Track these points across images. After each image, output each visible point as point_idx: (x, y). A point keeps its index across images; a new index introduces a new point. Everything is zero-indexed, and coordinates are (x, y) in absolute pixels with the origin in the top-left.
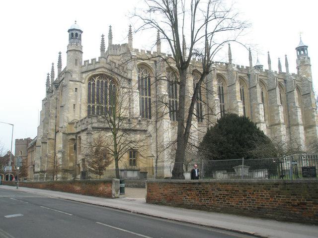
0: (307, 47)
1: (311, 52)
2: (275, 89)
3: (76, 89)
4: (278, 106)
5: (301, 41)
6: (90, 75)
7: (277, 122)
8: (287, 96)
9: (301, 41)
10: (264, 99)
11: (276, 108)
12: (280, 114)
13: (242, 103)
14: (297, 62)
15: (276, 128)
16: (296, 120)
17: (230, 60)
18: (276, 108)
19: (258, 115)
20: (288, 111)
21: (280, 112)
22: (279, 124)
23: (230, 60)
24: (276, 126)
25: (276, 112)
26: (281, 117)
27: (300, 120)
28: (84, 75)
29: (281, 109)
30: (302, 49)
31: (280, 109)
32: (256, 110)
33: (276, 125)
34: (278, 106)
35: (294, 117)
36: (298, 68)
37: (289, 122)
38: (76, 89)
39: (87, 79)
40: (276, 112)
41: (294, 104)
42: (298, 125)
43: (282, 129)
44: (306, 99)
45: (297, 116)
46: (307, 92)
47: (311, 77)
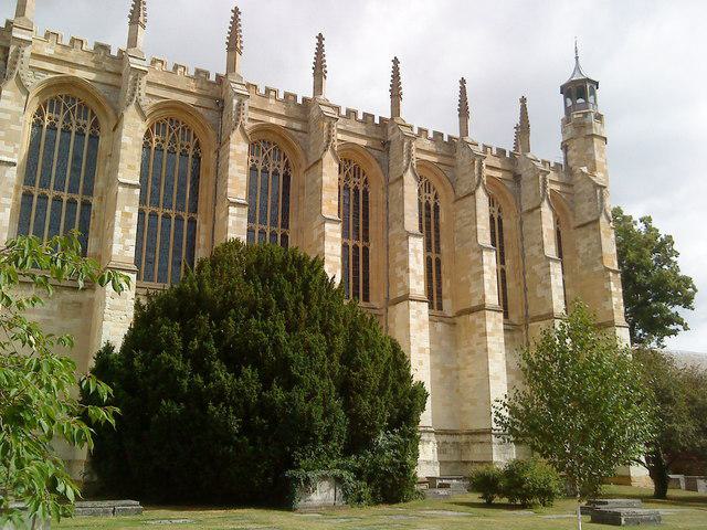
0: (597, 84)
1: (603, 100)
4: (481, 249)
5: (577, 67)
7: (475, 303)
8: (521, 223)
9: (577, 67)
11: (474, 256)
12: (487, 277)
13: (338, 227)
14: (563, 126)
15: (474, 322)
16: (547, 300)
17: (318, 88)
18: (474, 256)
19: (403, 273)
20: (524, 273)
21: (486, 268)
22: (482, 308)
23: (318, 88)
25: (475, 270)
26: (487, 286)
30: (578, 91)
32: (399, 257)
33: (471, 311)
34: (481, 249)
35: (540, 292)
36: (565, 147)
37: (527, 307)
41: (542, 251)
43: (489, 326)
44: (586, 241)
45: (548, 287)
46: (589, 219)
47: (605, 172)
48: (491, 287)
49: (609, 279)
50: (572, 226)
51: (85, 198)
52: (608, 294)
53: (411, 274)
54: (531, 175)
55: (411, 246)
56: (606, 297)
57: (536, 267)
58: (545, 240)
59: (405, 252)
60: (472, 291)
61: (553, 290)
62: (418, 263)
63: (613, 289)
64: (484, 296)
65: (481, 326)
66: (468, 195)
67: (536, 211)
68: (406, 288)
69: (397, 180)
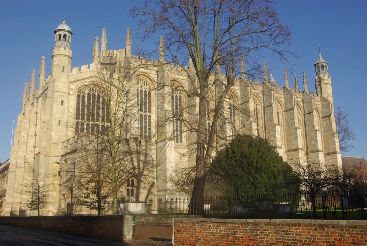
2: (293, 109)
3: (62, 102)
4: (296, 129)
6: (80, 85)
10: (280, 120)
11: (293, 131)
12: (299, 139)
16: (316, 145)
21: (298, 136)
22: (297, 149)
24: (293, 152)
26: (299, 142)
27: (320, 147)
28: (73, 86)
29: (300, 132)
31: (298, 133)
38: (62, 102)
39: (76, 90)
40: (294, 136)
42: (317, 151)
45: (316, 141)
48: (300, 142)
49: (334, 137)
50: (321, 116)
51: (145, 113)
52: (334, 142)
53: (277, 139)
54: (308, 100)
55: (277, 130)
56: (334, 143)
57: (312, 134)
58: (315, 124)
59: (274, 131)
60: (293, 143)
61: (318, 141)
62: (279, 135)
63: (336, 140)
64: (298, 145)
65: (297, 156)
66: (291, 109)
67: (311, 114)
68: (276, 144)
69: (270, 106)
